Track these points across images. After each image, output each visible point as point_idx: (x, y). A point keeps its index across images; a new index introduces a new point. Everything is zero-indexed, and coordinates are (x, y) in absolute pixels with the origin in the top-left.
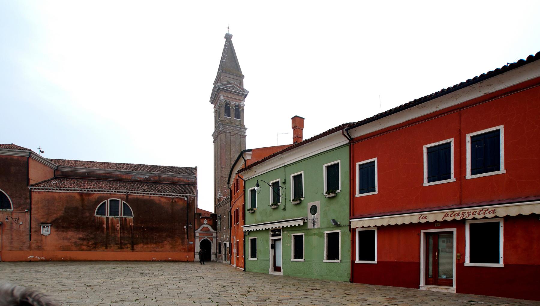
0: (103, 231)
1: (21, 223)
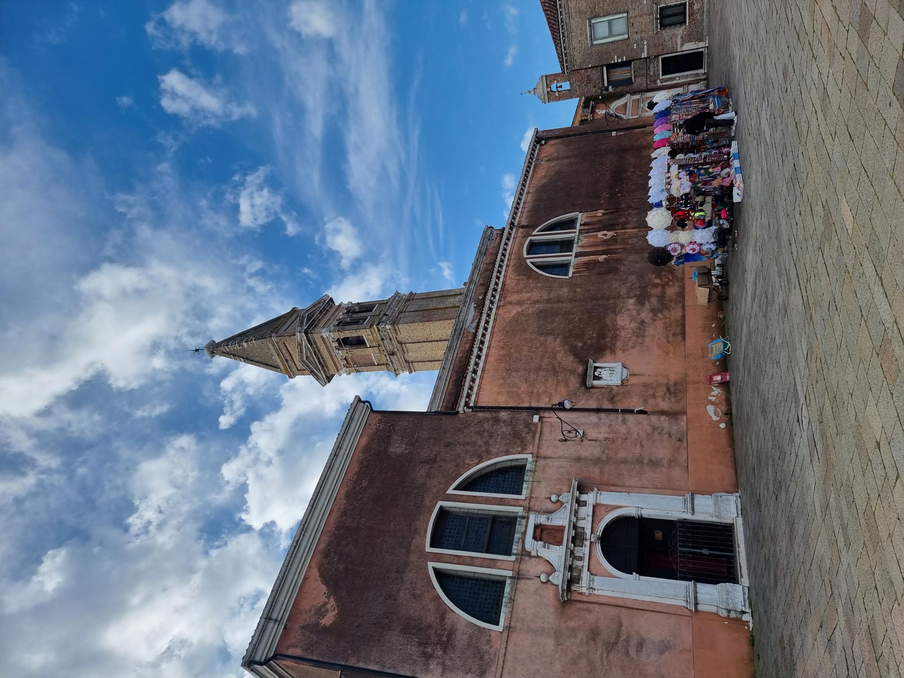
0: (618, 261)
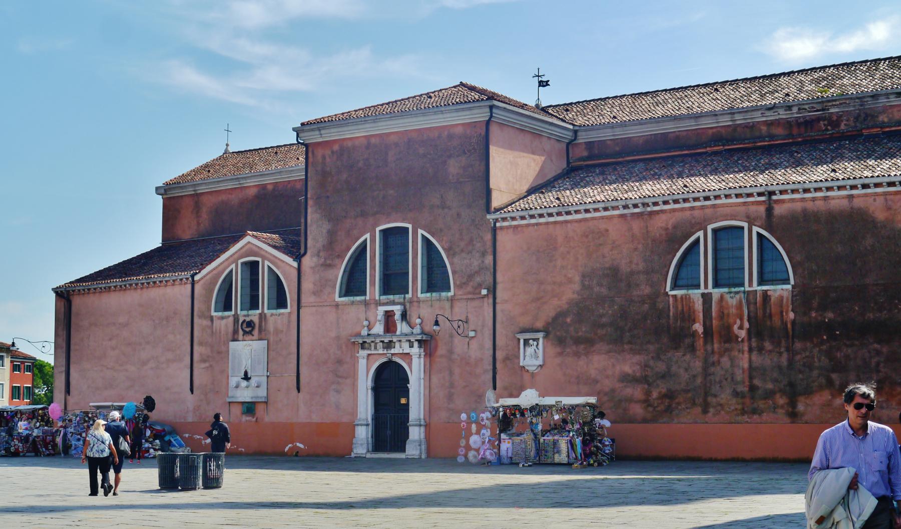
0: (692, 348)
1: (472, 334)
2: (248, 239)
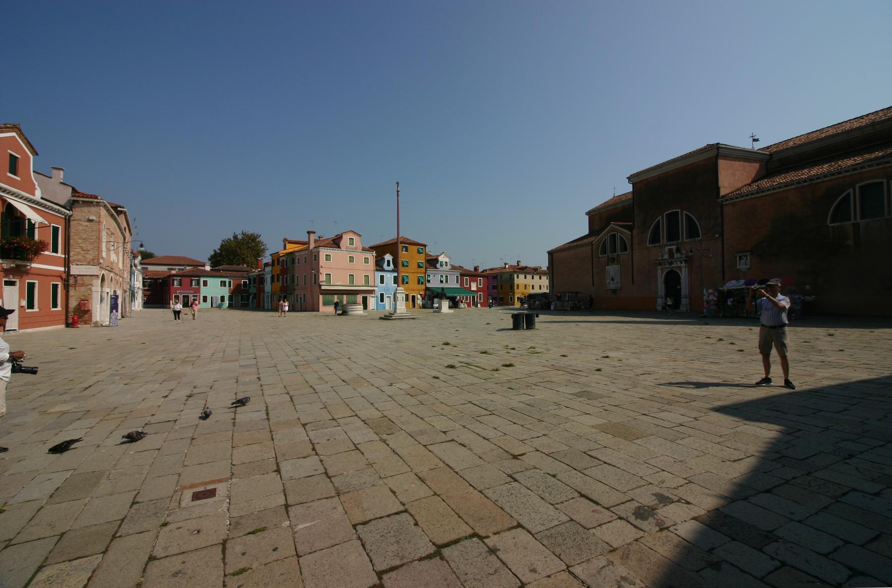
1: (711, 256)
2: (611, 225)
